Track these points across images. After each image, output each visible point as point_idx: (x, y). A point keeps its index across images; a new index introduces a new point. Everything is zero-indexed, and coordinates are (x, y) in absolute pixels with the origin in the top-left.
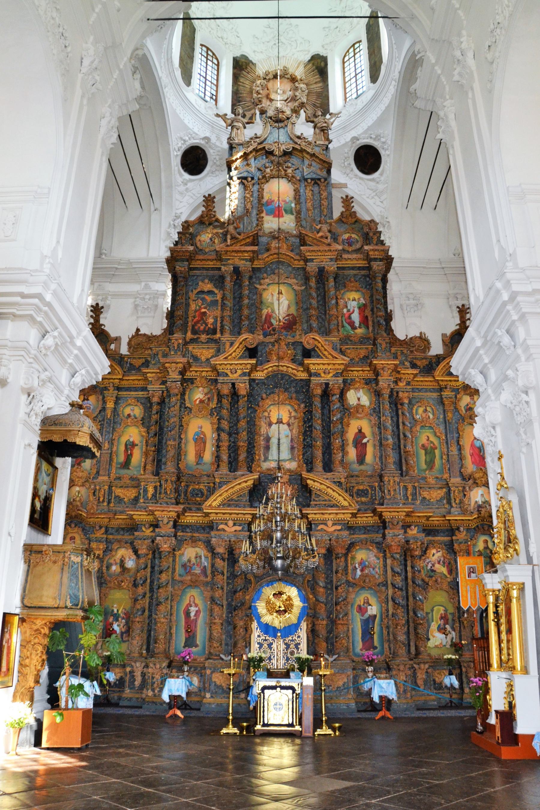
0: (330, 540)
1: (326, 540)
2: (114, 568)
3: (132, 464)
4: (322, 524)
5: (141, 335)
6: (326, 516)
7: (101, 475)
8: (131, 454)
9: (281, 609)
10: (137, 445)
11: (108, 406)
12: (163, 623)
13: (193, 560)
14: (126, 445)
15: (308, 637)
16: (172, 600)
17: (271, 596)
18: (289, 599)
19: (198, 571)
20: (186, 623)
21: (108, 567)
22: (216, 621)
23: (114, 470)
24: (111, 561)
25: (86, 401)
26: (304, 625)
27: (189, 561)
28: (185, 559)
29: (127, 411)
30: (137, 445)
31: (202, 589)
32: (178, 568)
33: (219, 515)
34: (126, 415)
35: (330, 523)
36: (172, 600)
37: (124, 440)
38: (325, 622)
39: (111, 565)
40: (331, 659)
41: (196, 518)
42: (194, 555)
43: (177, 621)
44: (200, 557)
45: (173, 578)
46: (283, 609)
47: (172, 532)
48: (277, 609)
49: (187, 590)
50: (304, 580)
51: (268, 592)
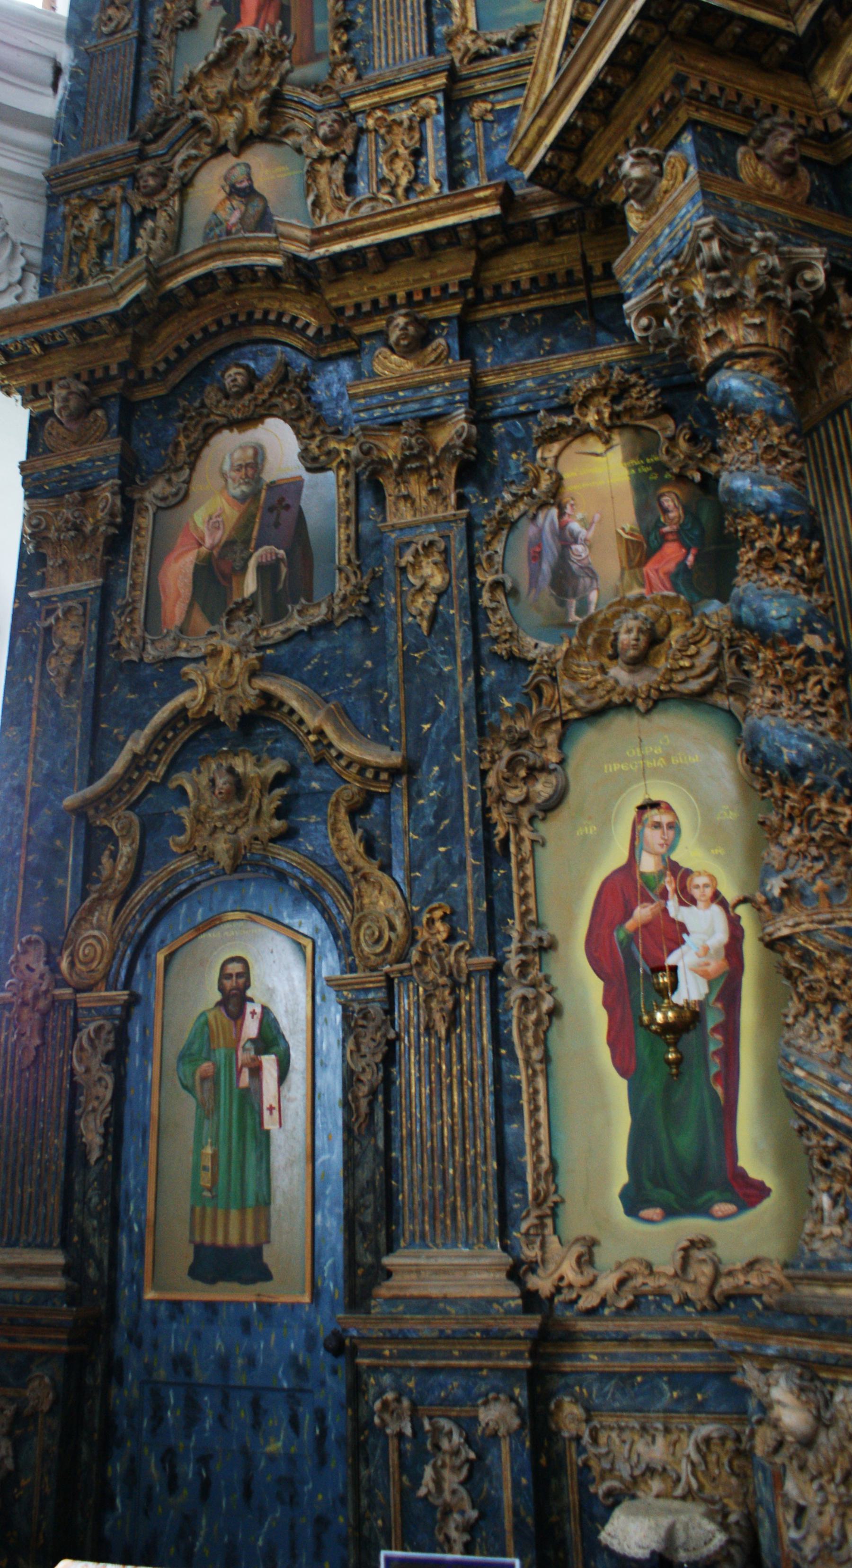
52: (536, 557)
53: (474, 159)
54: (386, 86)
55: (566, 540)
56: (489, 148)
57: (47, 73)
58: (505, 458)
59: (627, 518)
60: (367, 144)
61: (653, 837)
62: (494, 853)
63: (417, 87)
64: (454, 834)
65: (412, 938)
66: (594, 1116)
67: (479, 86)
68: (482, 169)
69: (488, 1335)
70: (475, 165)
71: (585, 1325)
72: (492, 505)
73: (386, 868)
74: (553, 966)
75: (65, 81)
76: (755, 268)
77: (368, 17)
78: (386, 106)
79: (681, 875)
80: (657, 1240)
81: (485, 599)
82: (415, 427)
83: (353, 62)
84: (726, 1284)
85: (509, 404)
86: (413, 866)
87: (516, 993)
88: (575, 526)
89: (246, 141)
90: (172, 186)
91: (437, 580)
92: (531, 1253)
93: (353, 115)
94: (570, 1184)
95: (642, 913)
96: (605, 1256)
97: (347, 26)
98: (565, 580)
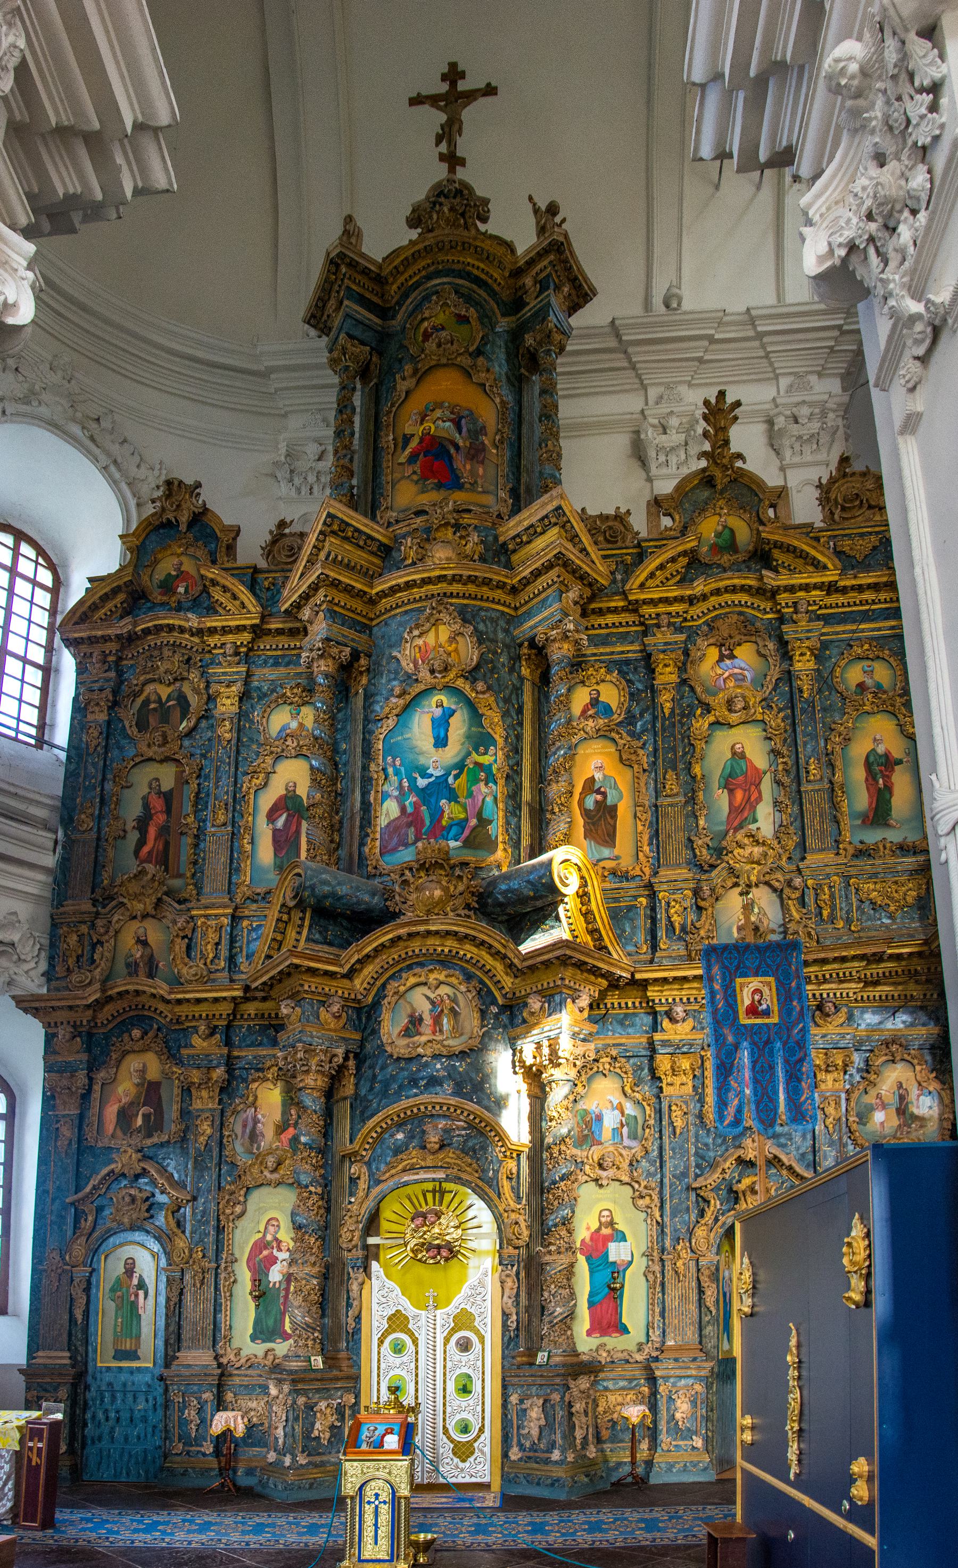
2: (879, 1116)
3: (894, 813)
5: (853, 474)
7: (814, 851)
8: (889, 788)
10: (899, 762)
11: (798, 666)
14: (868, 765)
21: (863, 1118)
23: (847, 835)
24: (870, 1099)
25: (728, 662)
29: (854, 675)
30: (899, 762)
34: (853, 686)
37: (860, 749)
39: (871, 1109)
52: (245, 1126)
53: (241, 948)
54: (206, 908)
55: (256, 1121)
56: (248, 942)
57: (50, 844)
58: (238, 1086)
59: (277, 1116)
60: (198, 934)
61: (271, 1229)
62: (220, 1230)
63: (220, 911)
64: (208, 1222)
65: (191, 1257)
66: (243, 1314)
67: (247, 913)
68: (244, 953)
69: (205, 1375)
70: (241, 951)
71: (236, 1372)
72: (231, 1105)
73: (184, 1232)
74: (236, 1265)
75: (59, 848)
76: (317, 1058)
77: (204, 859)
78: (206, 916)
79: (279, 1242)
80: (259, 1349)
81: (225, 1140)
82: (205, 1071)
83: (195, 885)
84: (277, 1361)
85: (242, 1064)
86: (192, 1233)
87: (222, 1276)
88: (260, 1116)
89: (145, 916)
90: (112, 933)
91: (209, 1131)
92: (221, 1352)
93: (192, 917)
94: (234, 1332)
95: (265, 1253)
96: (243, 1353)
97: (195, 863)
98: (254, 1137)
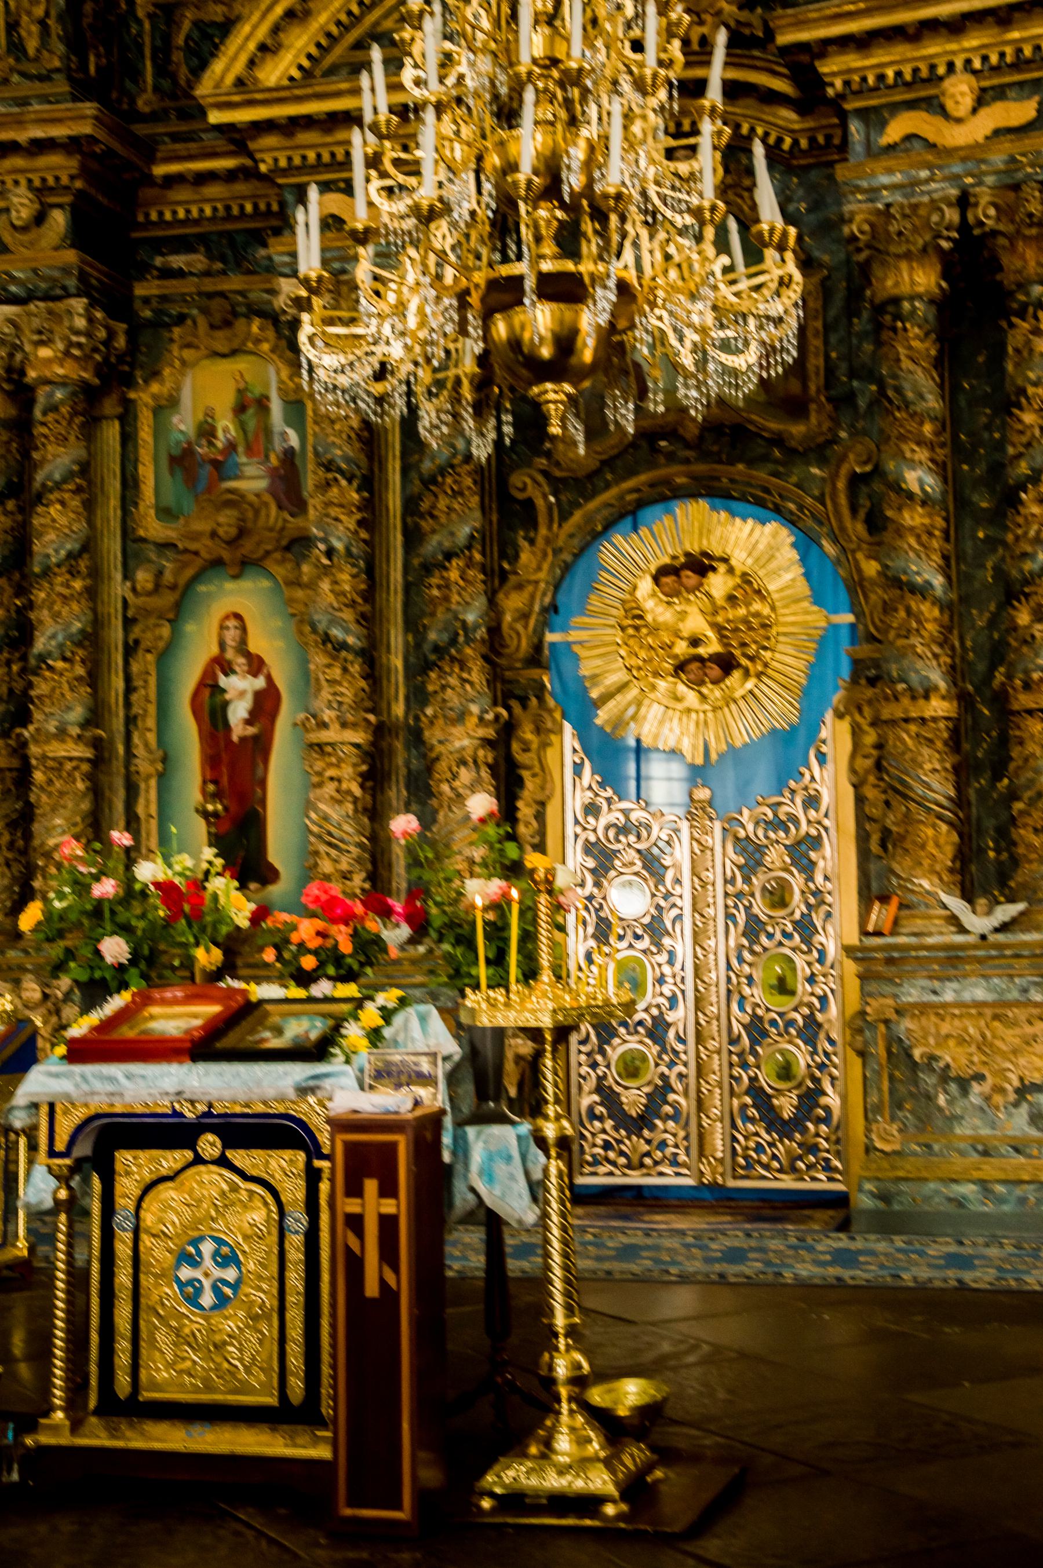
0: (964, 201)
1: (935, 206)
4: (911, 105)
6: (934, 48)
9: (702, 651)
12: (60, 762)
13: (226, 426)
15: (860, 800)
16: (130, 650)
17: (645, 585)
18: (748, 587)
19: (253, 480)
20: (212, 761)
22: (325, 736)
26: (835, 735)
27: (207, 431)
28: (183, 424)
31: (281, 572)
32: (147, 472)
33: (305, 137)
35: (960, 91)
36: (130, 650)
38: (939, 707)
40: (978, 923)
41: (213, 190)
42: (223, 402)
43: (166, 759)
44: (262, 404)
45: (128, 534)
46: (712, 647)
47: (66, 270)
48: (681, 648)
49: (202, 588)
50: (834, 477)
51: (632, 557)
